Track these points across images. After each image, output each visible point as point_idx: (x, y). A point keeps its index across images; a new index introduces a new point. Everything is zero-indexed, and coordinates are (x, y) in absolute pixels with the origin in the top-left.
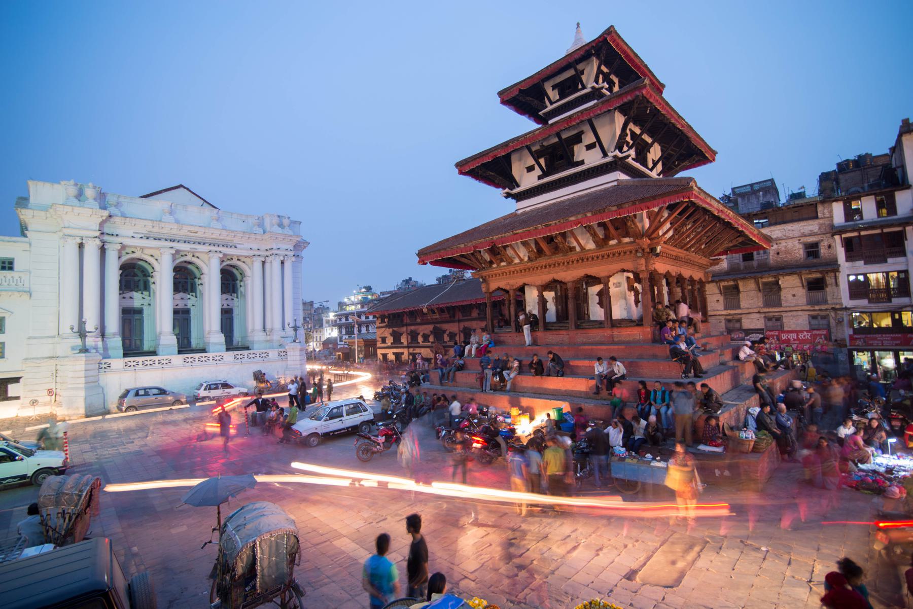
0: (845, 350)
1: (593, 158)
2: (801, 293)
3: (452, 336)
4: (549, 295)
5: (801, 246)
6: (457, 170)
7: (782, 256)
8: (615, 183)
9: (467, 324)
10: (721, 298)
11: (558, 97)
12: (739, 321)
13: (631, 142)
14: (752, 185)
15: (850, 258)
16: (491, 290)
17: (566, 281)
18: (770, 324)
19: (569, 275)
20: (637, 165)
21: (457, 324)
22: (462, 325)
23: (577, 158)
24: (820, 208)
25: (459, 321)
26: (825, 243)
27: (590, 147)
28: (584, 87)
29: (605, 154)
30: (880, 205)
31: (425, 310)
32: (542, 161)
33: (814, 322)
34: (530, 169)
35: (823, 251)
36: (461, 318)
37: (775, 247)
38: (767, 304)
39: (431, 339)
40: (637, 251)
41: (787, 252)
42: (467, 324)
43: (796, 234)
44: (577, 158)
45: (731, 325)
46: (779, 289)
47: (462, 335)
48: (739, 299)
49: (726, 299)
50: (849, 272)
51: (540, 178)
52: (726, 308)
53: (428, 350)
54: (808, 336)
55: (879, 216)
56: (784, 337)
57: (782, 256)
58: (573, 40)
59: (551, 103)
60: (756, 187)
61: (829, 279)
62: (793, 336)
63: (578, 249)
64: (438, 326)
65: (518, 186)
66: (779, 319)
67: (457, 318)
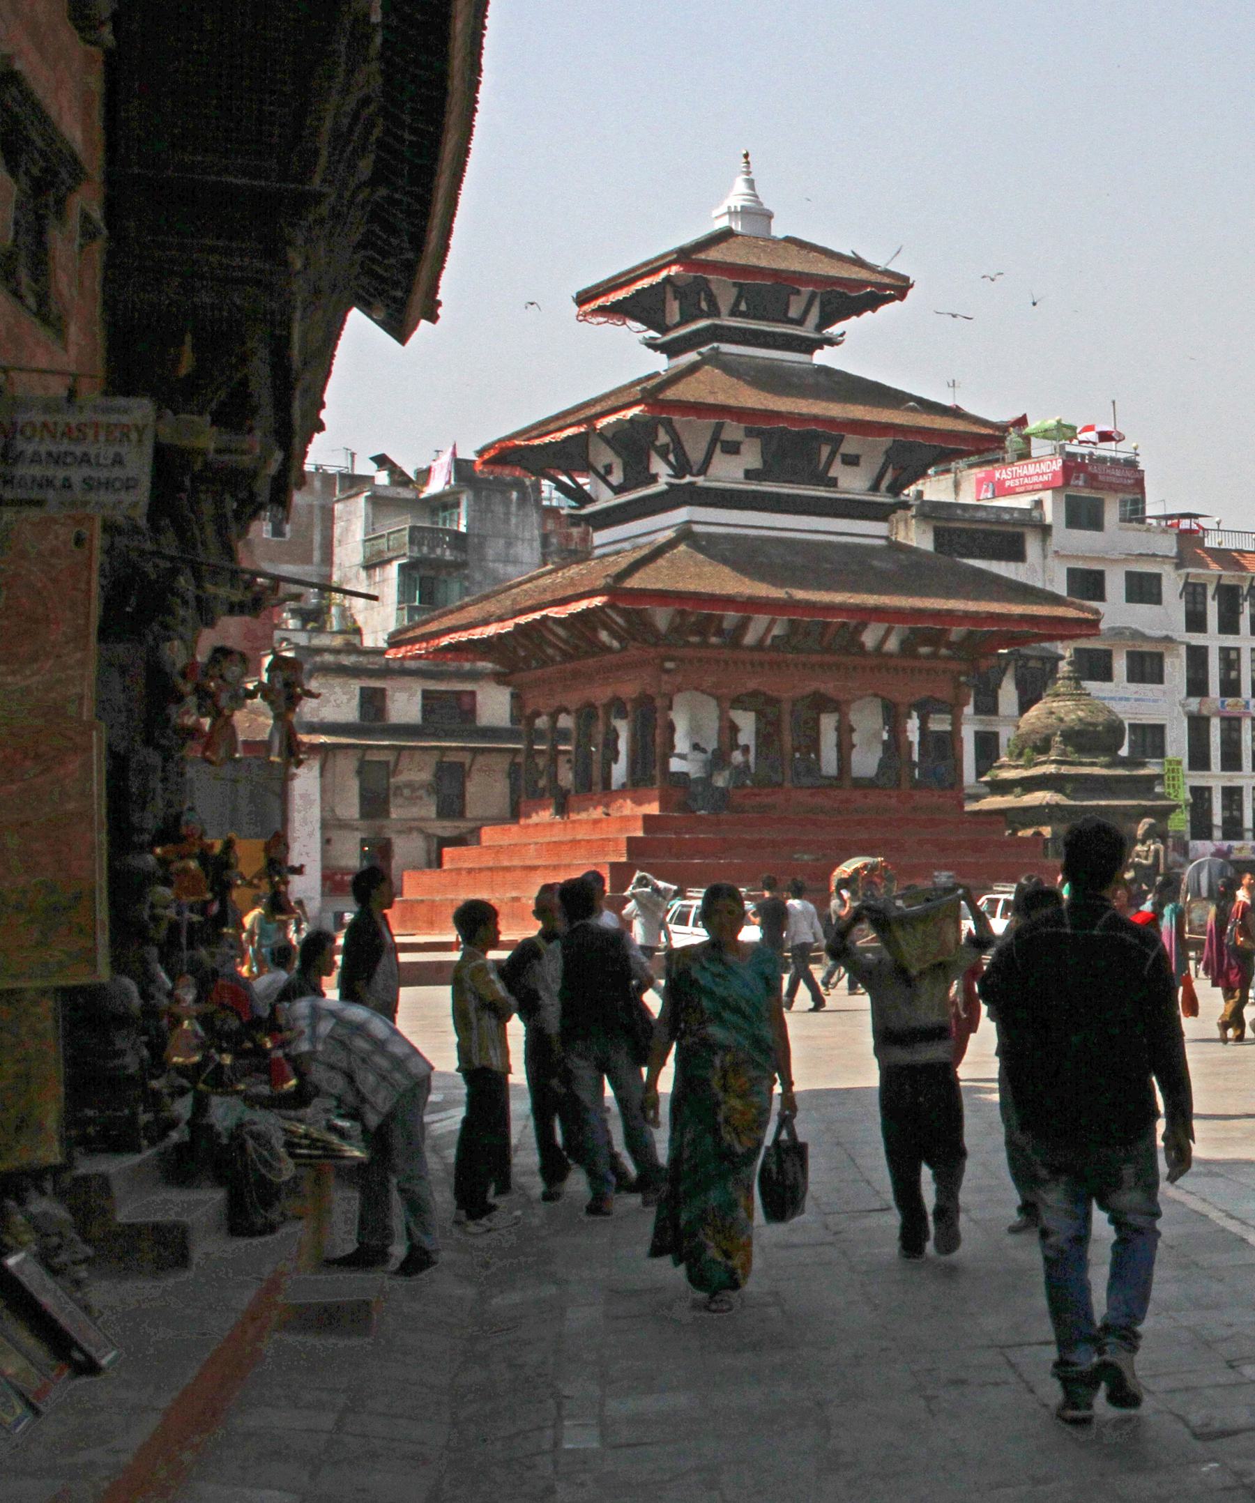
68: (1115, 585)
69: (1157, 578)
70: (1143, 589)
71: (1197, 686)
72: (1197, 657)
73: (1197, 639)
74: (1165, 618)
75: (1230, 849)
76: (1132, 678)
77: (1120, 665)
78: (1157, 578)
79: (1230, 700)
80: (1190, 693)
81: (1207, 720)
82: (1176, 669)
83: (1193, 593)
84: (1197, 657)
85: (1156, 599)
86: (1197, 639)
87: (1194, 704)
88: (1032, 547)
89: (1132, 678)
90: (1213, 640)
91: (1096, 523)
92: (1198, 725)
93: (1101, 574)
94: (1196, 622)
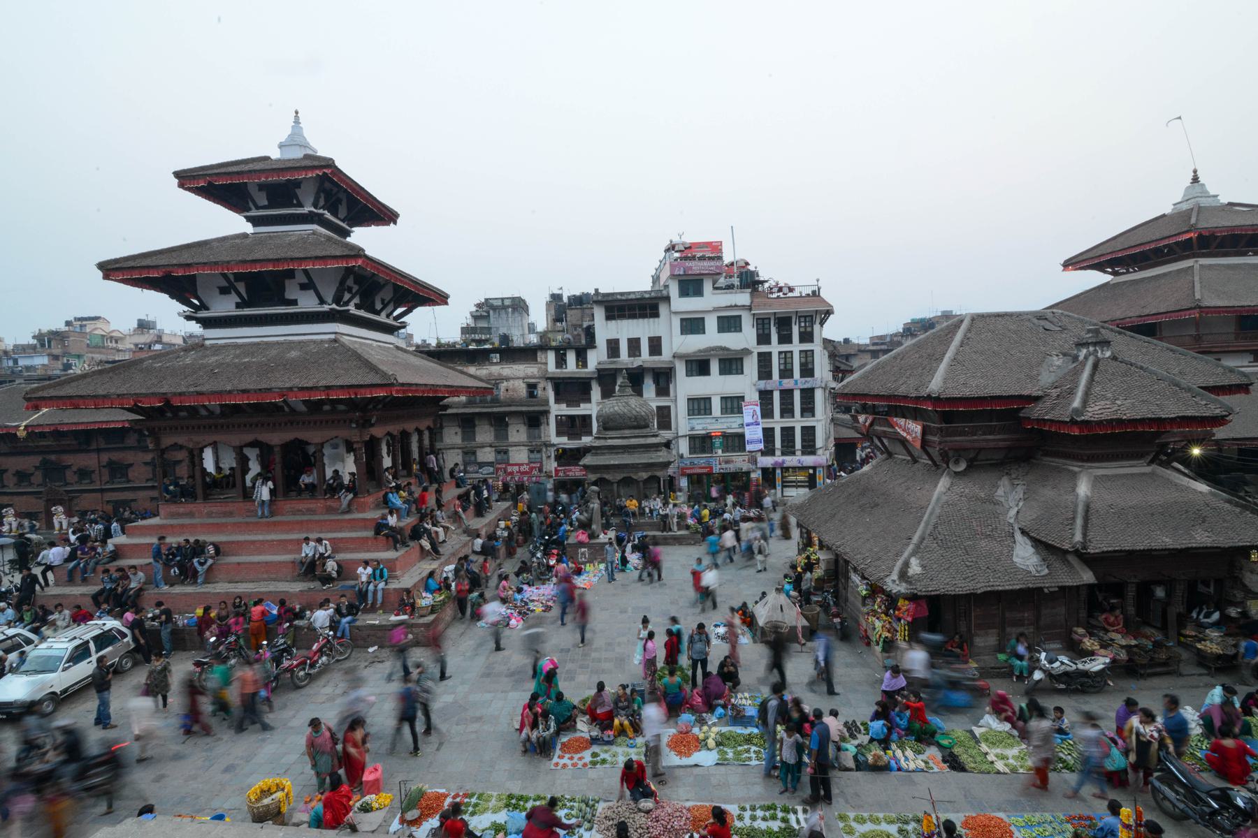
0: (551, 481)
1: (308, 303)
2: (523, 429)
3: (83, 474)
4: (252, 454)
5: (524, 386)
6: (100, 274)
7: (510, 393)
8: (333, 336)
9: (116, 456)
10: (459, 430)
11: (266, 203)
12: (474, 453)
13: (355, 288)
14: (503, 299)
15: (557, 401)
16: (163, 446)
17: (273, 443)
18: (499, 457)
19: (276, 438)
20: (362, 313)
21: (94, 455)
22: (105, 457)
23: (289, 295)
24: (539, 354)
25: (99, 451)
26: (540, 386)
27: (304, 287)
28: (300, 205)
29: (322, 302)
30: (577, 360)
31: (21, 433)
32: (241, 287)
33: (532, 456)
34: (224, 291)
35: (539, 392)
36: (103, 446)
37: (505, 384)
38: (497, 437)
39: (38, 477)
40: (351, 421)
41: (514, 390)
42: (116, 456)
43: (521, 374)
44: (289, 295)
45: (467, 459)
46: (507, 425)
47: (106, 472)
48: (474, 433)
49: (463, 433)
50: (558, 410)
51: (238, 306)
52: (463, 440)
53: (32, 499)
54: (526, 468)
55: (577, 366)
56: (509, 469)
57: (510, 393)
58: (289, 131)
59: (258, 208)
60: (507, 303)
61: (543, 420)
62: (516, 469)
63: (286, 409)
64: (53, 457)
65: (207, 309)
66: (506, 452)
67: (94, 446)
68: (711, 323)
69: (740, 317)
70: (729, 324)
71: (765, 373)
72: (764, 359)
73: (764, 349)
74: (745, 338)
75: (784, 462)
76: (723, 371)
77: (714, 367)
78: (740, 317)
79: (785, 381)
80: (760, 378)
81: (771, 392)
82: (751, 366)
83: (762, 325)
84: (764, 359)
85: (738, 328)
86: (764, 349)
87: (763, 385)
88: (663, 309)
89: (723, 371)
90: (775, 348)
91: (699, 292)
92: (765, 396)
93: (703, 319)
94: (763, 338)
